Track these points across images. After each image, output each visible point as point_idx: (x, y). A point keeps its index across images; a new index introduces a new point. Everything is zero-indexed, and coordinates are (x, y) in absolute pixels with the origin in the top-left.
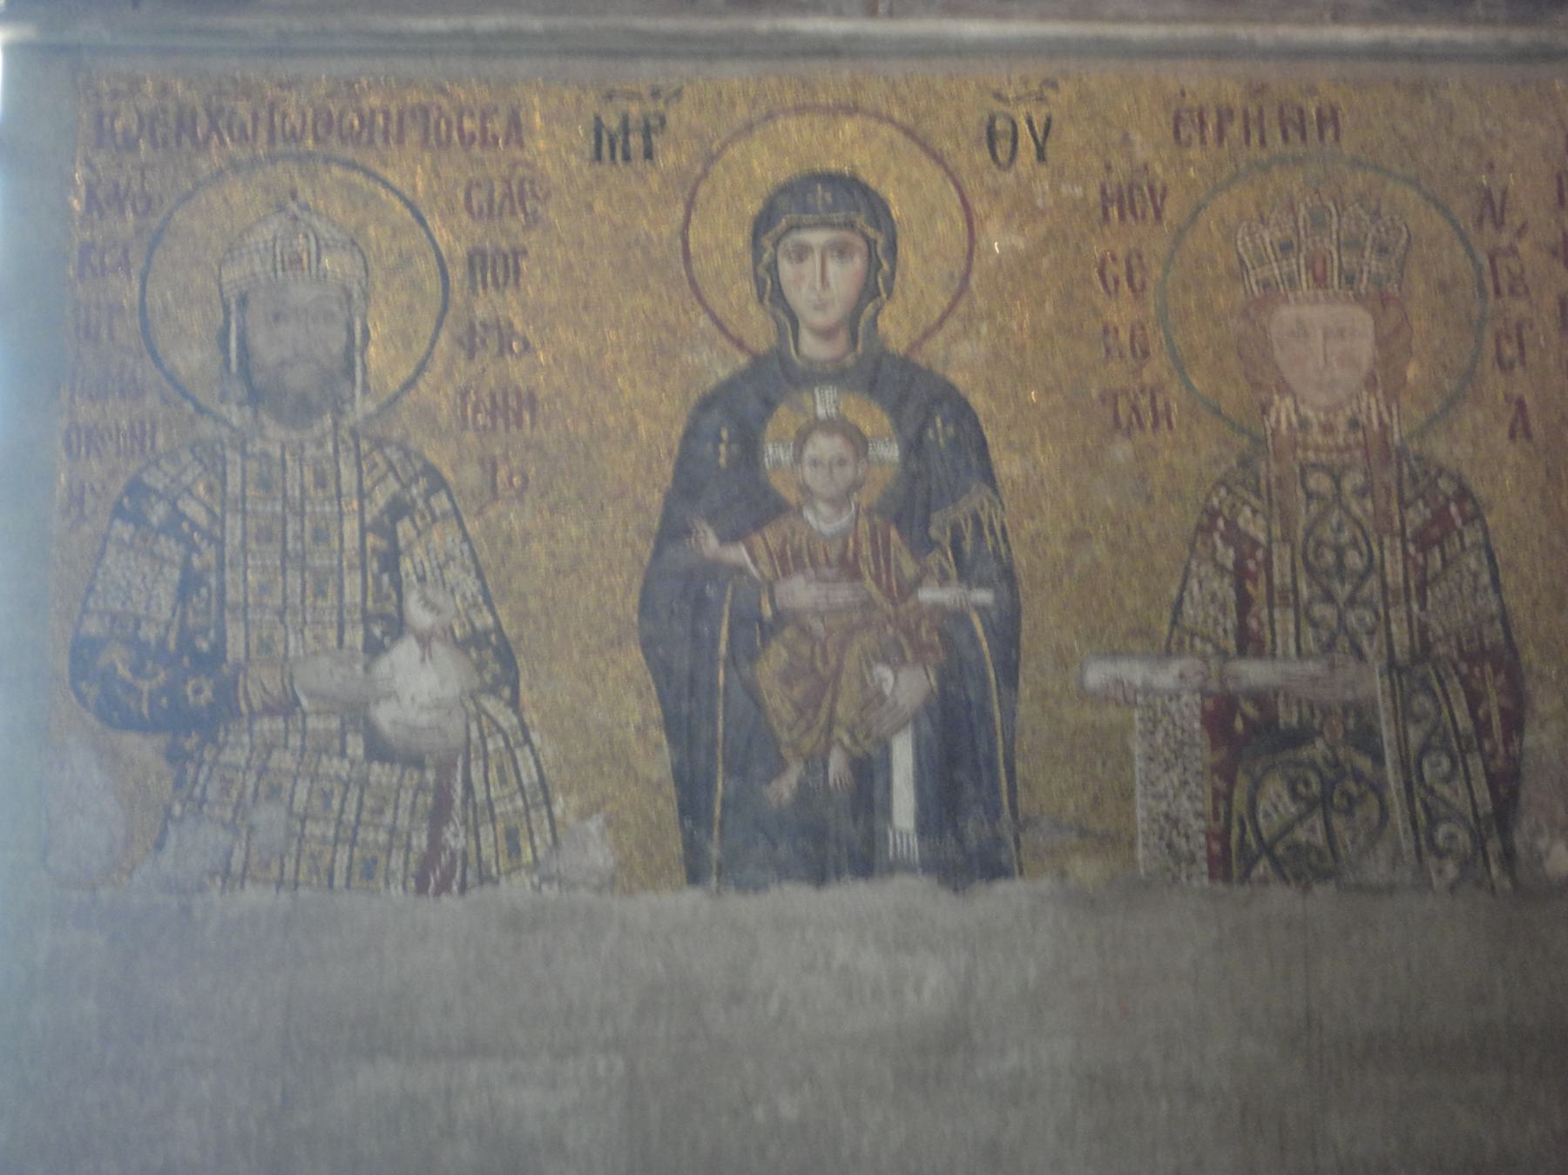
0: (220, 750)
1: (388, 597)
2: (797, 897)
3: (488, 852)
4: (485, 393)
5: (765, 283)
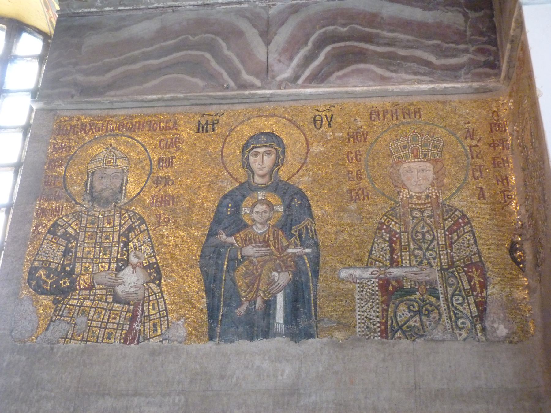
0: (69, 300)
1: (125, 255)
2: (244, 345)
3: (147, 331)
5: (245, 162)
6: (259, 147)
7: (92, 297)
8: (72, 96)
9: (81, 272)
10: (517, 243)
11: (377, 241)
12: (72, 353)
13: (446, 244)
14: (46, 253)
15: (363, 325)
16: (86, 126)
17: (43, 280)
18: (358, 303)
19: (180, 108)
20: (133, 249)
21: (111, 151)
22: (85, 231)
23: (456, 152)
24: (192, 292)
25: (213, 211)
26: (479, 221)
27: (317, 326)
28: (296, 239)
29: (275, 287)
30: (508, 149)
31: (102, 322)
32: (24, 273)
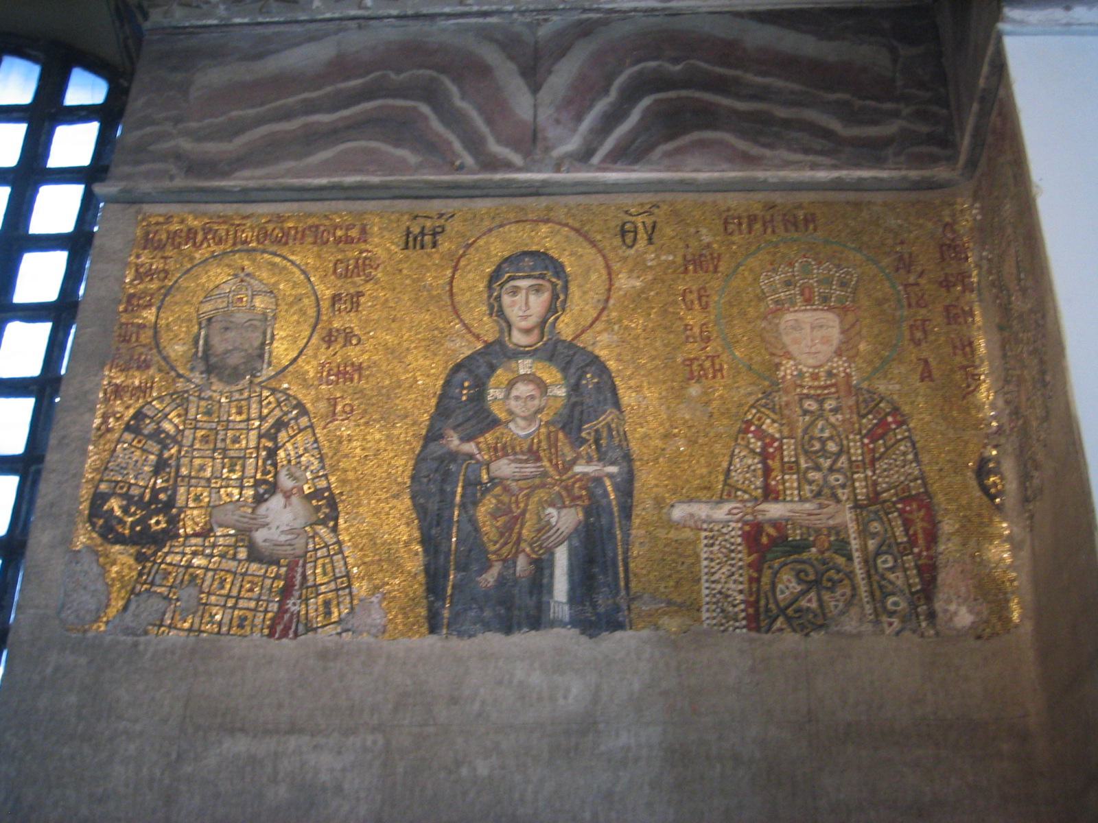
0: (167, 554)
1: (269, 472)
2: (494, 641)
3: (312, 614)
4: (334, 365)
6: (520, 278)
7: (208, 551)
8: (172, 178)
10: (989, 459)
12: (173, 653)
13: (863, 461)
14: (122, 468)
15: (714, 607)
16: (196, 233)
17: (117, 517)
18: (706, 567)
19: (373, 203)
20: (285, 463)
21: (242, 281)
23: (879, 295)
26: (923, 419)
27: (629, 609)
29: (550, 537)
30: (972, 291)
31: (228, 596)
32: (81, 503)
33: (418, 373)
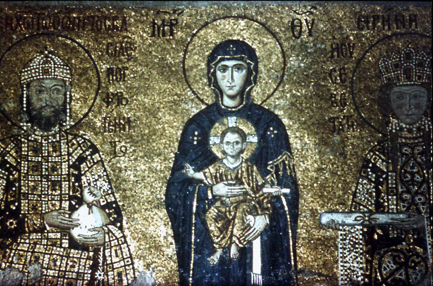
1: (78, 191)
5: (211, 79)
9: (28, 211)
11: (362, 181)
15: (346, 277)
16: (12, 19)
18: (341, 253)
20: (87, 184)
22: (28, 161)
24: (159, 237)
25: (177, 139)
27: (297, 277)
28: (273, 176)
33: (166, 125)
